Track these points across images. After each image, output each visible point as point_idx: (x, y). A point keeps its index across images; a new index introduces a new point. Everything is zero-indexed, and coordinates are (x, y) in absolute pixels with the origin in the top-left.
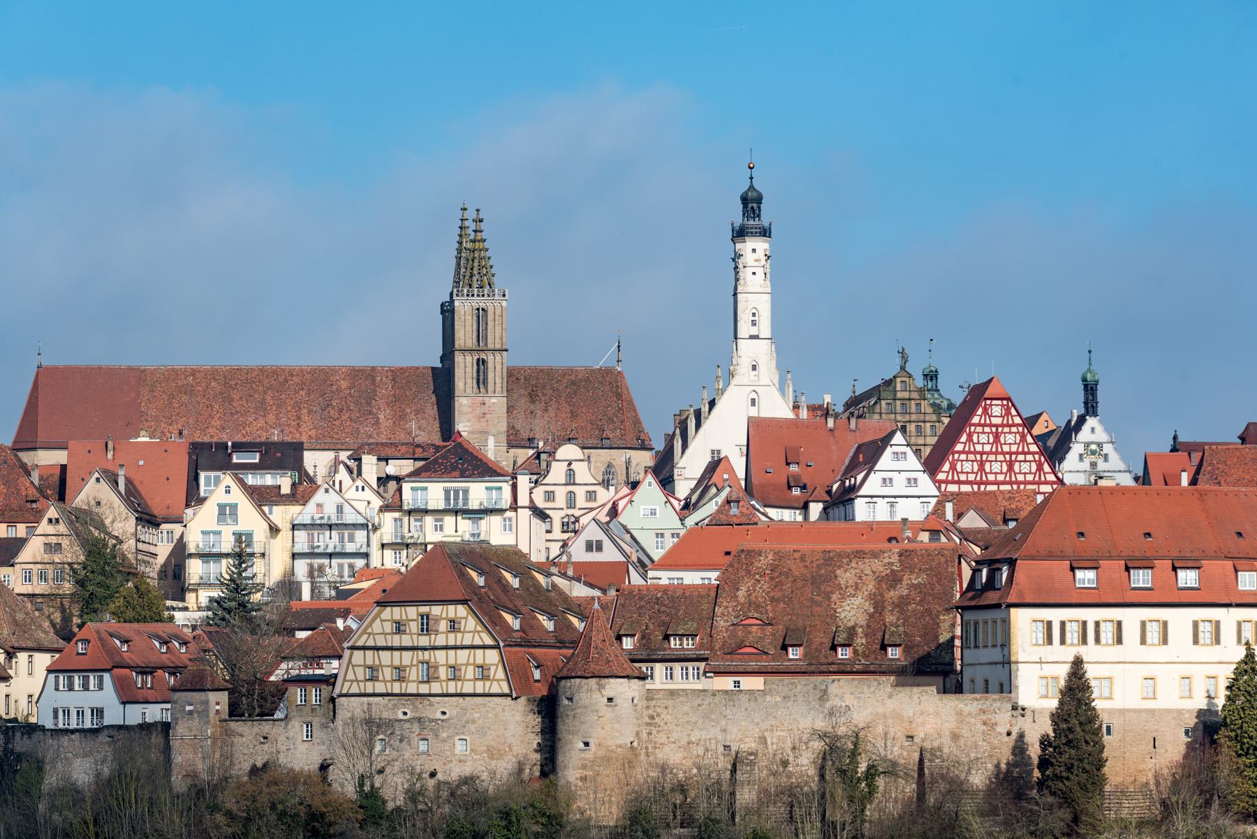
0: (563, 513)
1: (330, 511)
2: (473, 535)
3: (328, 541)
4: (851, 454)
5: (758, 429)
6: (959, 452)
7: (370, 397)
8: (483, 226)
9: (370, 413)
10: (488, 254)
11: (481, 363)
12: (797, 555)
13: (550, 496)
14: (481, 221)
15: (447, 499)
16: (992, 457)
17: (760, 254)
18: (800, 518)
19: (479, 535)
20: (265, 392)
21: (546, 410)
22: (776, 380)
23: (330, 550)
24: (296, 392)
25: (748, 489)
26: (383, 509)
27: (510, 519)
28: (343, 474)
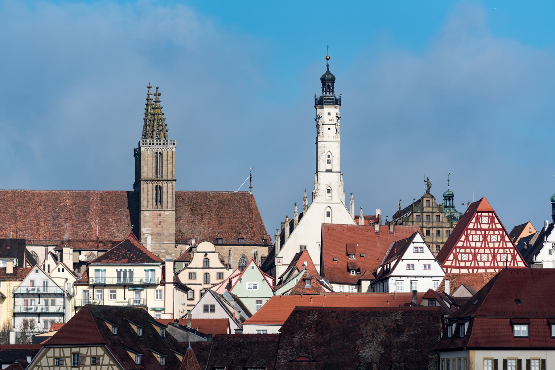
0: (201, 287)
1: (39, 284)
2: (136, 301)
3: (38, 305)
4: (390, 249)
5: (329, 232)
6: (460, 248)
7: (85, 211)
8: (160, 98)
9: (86, 221)
10: (164, 117)
11: (159, 189)
12: (333, 315)
13: (193, 276)
14: (159, 95)
15: (119, 277)
16: (482, 251)
17: (333, 116)
18: (355, 291)
19: (139, 301)
20: (16, 207)
21: (202, 220)
22: (343, 200)
23: (39, 311)
24: (37, 207)
25: (322, 274)
26: (77, 283)
27: (160, 291)
28: (50, 261)
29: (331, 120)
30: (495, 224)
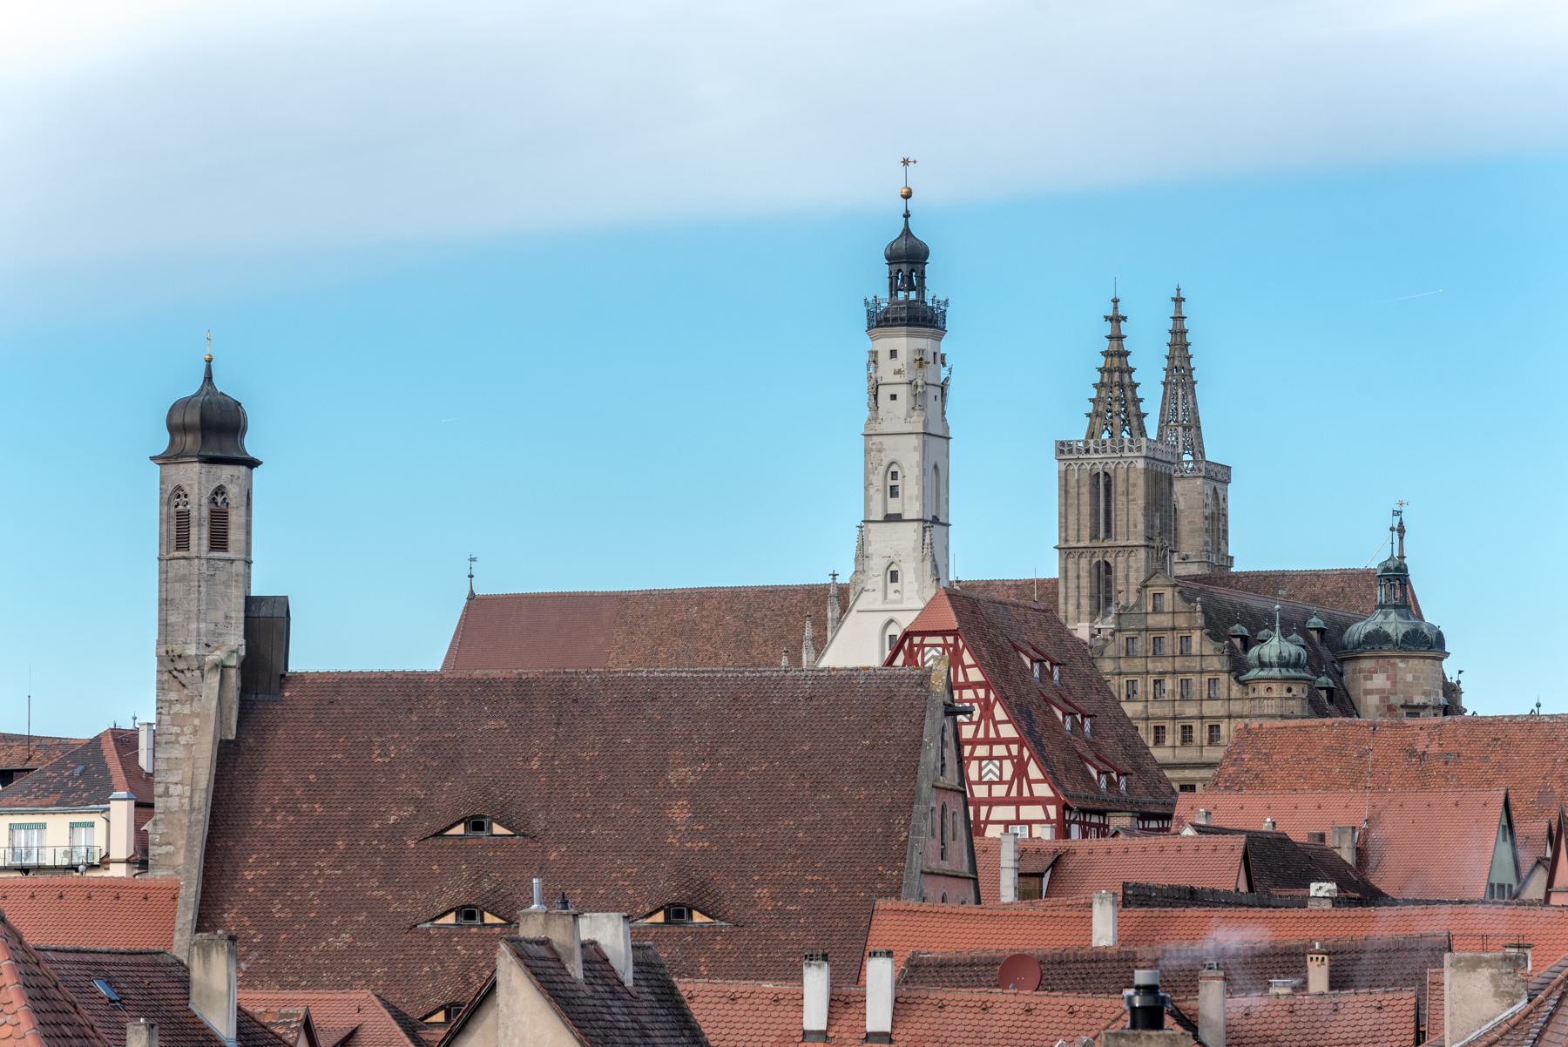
29: (898, 372)
30: (964, 668)
